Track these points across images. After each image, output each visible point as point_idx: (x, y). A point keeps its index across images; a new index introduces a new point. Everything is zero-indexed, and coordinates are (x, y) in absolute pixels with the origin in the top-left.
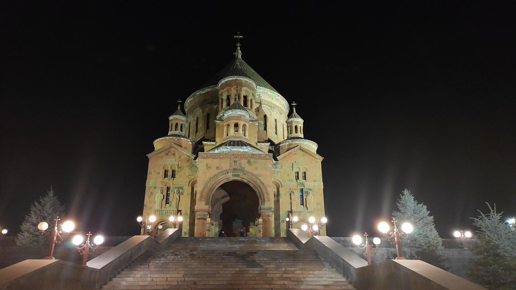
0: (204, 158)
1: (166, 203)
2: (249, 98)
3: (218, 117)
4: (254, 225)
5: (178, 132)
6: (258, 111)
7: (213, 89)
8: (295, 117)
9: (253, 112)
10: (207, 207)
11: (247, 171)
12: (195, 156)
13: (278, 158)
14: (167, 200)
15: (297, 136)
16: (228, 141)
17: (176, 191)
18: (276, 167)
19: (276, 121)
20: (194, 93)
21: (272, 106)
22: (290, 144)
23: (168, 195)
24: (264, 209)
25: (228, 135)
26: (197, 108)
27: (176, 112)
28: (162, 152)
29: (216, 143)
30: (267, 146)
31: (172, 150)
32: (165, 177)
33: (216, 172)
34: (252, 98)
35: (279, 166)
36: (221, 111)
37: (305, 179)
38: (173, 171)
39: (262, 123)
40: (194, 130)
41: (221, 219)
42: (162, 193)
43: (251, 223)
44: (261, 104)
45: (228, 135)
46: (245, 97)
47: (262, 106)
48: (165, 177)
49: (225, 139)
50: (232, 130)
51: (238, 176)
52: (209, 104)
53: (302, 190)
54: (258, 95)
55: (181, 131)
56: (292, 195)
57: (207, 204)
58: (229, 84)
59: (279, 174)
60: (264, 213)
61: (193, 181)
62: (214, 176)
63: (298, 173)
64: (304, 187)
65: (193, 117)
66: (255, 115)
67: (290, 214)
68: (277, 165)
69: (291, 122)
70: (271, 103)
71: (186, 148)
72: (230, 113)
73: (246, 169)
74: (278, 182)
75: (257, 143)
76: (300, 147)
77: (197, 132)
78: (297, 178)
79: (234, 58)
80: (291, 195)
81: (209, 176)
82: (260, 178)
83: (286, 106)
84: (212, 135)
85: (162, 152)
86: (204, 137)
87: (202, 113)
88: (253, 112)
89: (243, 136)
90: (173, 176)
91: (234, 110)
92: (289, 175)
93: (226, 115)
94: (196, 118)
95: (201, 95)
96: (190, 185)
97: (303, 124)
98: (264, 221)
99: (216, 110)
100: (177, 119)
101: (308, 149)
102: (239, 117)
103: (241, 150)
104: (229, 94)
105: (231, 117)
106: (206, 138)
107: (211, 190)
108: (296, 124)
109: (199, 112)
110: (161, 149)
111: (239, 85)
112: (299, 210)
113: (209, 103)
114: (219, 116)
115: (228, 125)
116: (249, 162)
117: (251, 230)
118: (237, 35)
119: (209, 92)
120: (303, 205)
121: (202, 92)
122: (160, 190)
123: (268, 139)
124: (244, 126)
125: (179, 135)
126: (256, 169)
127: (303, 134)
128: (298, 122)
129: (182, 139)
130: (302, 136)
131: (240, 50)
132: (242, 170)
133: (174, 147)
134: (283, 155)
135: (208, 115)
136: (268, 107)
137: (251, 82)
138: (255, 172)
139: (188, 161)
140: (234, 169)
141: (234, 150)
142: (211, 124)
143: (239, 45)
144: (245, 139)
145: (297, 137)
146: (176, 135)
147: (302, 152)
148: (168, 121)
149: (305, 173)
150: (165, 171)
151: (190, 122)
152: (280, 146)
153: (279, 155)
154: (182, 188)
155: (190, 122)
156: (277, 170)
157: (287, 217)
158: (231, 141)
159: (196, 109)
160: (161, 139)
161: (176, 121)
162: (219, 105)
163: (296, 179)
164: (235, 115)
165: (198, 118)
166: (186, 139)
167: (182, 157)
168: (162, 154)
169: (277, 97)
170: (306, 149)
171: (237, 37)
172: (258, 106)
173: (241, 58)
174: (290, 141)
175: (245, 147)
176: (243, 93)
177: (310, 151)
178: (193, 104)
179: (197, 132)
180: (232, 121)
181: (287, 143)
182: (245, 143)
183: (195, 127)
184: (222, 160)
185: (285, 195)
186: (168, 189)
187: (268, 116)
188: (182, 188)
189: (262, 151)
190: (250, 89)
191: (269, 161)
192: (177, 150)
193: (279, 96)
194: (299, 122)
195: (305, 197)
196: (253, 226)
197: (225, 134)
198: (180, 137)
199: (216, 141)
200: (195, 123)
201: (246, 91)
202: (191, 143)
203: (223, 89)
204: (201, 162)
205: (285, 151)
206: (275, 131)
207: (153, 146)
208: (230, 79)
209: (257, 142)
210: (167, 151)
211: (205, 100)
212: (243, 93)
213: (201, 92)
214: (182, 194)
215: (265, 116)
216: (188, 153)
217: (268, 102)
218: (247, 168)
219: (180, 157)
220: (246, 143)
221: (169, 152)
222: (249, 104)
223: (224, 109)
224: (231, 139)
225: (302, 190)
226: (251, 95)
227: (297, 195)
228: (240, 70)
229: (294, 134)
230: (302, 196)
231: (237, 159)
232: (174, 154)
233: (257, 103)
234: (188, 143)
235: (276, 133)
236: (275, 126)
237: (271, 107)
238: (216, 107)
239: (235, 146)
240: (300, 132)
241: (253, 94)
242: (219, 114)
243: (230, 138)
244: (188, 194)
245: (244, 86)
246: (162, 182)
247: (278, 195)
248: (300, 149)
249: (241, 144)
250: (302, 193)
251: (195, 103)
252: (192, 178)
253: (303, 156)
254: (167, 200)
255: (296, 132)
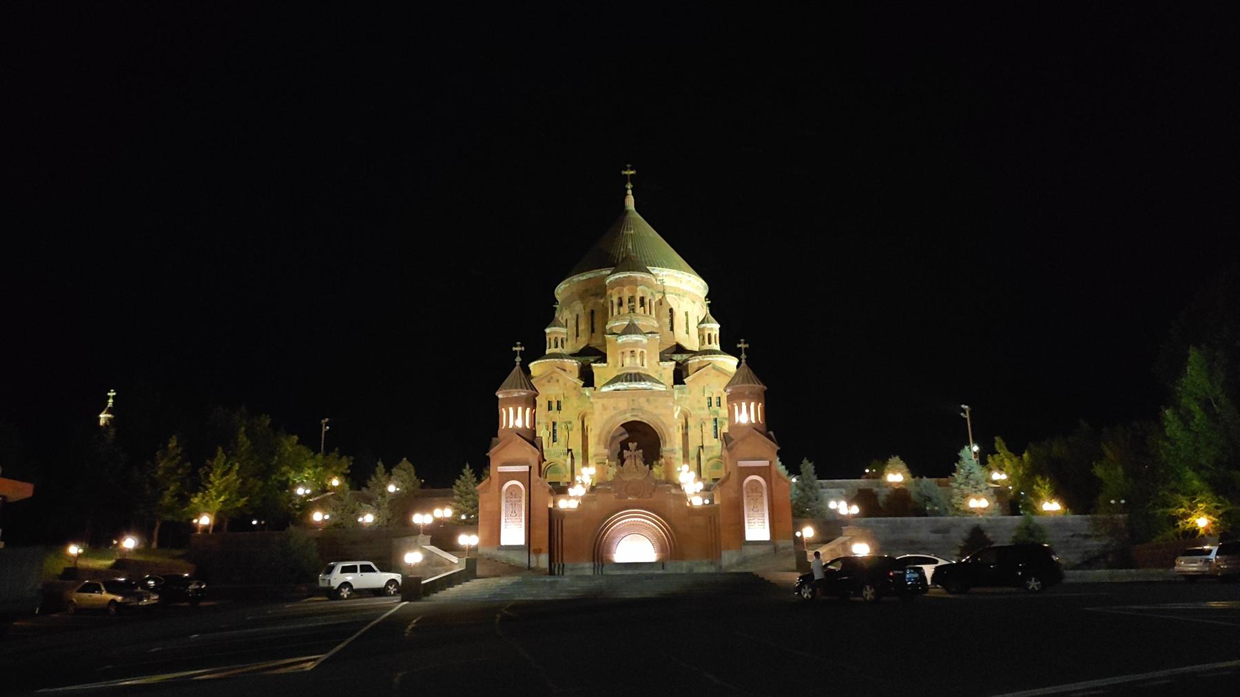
0: (600, 398)
1: (554, 441)
2: (647, 301)
3: (608, 327)
4: (658, 464)
5: (558, 350)
6: (661, 304)
7: (598, 275)
8: (708, 323)
9: (653, 318)
10: (606, 451)
11: (646, 411)
12: (583, 382)
13: (685, 380)
14: (554, 436)
15: (711, 348)
16: (624, 374)
17: (563, 427)
18: (683, 393)
19: (686, 314)
20: (569, 279)
21: (680, 294)
22: (700, 362)
23: (554, 431)
24: (666, 451)
25: (623, 366)
26: (576, 300)
27: (553, 322)
28: (543, 378)
29: (608, 365)
30: (672, 365)
31: (553, 375)
32: (549, 410)
33: (613, 413)
34: (651, 297)
35: (687, 391)
36: (610, 320)
37: (720, 406)
38: (558, 402)
39: (667, 320)
40: (573, 333)
41: (619, 458)
42: (547, 429)
43: (655, 462)
44: (664, 293)
45: (623, 366)
46: (642, 299)
47: (666, 296)
48: (549, 410)
49: (619, 371)
50: (628, 361)
51: (637, 416)
52: (592, 298)
53: (716, 420)
54: (660, 280)
55: (563, 347)
56: (703, 427)
57: (605, 448)
58: (619, 283)
59: (688, 402)
60: (664, 454)
61: (583, 413)
62: (612, 417)
63: (710, 398)
64: (718, 415)
65: (571, 314)
66: (656, 322)
67: (701, 450)
68: (684, 390)
69: (703, 328)
70: (679, 289)
71: (570, 372)
72: (624, 339)
73: (645, 409)
74: (687, 411)
75: (658, 363)
76: (714, 365)
77: (577, 336)
78: (710, 405)
79: (623, 210)
80: (702, 427)
81: (605, 417)
82: (661, 417)
83: (702, 287)
84: (599, 341)
85: (543, 378)
86: (588, 344)
87: (584, 309)
88: (653, 318)
89: (640, 366)
90: (559, 408)
91: (629, 336)
92: (699, 402)
93: (620, 341)
94: (575, 317)
95: (579, 282)
96: (580, 418)
97: (718, 330)
98: (666, 462)
99: (603, 305)
100: (556, 332)
101: (723, 367)
102: (636, 343)
103: (639, 386)
104: (620, 296)
105: (624, 344)
106: (592, 346)
107: (609, 432)
108: (709, 332)
109: (578, 307)
110: (540, 376)
111: (634, 283)
112: (712, 444)
113: (593, 295)
114: (610, 327)
115: (623, 353)
116: (648, 400)
117: (654, 469)
118: (626, 170)
119: (590, 278)
120: (717, 438)
121: (581, 278)
122: (544, 427)
123: (675, 344)
124: (642, 352)
125: (560, 354)
126: (656, 407)
127: (719, 345)
128: (712, 329)
129: (566, 360)
130: (717, 347)
131: (633, 194)
132: (641, 409)
133: (557, 373)
134: (691, 376)
135: (593, 312)
136: (675, 297)
137: (648, 277)
138: (655, 411)
139: (575, 389)
140: (633, 409)
141: (631, 386)
142: (596, 326)
143: (629, 186)
144: (645, 370)
145: (709, 350)
146: (557, 354)
147: (715, 372)
148: (545, 333)
149: (719, 398)
150: (549, 402)
151: (566, 320)
152: (687, 365)
153: (688, 376)
154: (570, 423)
155: (566, 320)
156: (684, 396)
157: (684, 463)
158: (627, 374)
159: (575, 302)
160: (539, 361)
161: (555, 336)
162: (606, 299)
163: (709, 407)
164: (631, 341)
165: (577, 316)
166: (570, 361)
167: (568, 384)
168: (543, 382)
169: (689, 279)
170: (722, 369)
171: (626, 173)
172: (660, 297)
173: (634, 209)
174: (700, 357)
175: (643, 383)
176: (639, 295)
177: (725, 370)
178: (569, 294)
179: (577, 336)
180: (627, 349)
181: (697, 360)
182: (643, 376)
183: (575, 329)
184: (620, 399)
185: (695, 427)
186: (554, 424)
187: (675, 310)
188: (570, 423)
189: (662, 384)
190: (648, 288)
191: (669, 398)
192: (561, 375)
193: (690, 276)
194: (714, 328)
195: (719, 429)
196: (657, 466)
197: (620, 364)
198: (562, 358)
199: (608, 361)
200: (574, 322)
201: (643, 291)
202: (576, 364)
203: (613, 289)
204: (597, 402)
205: (695, 370)
206: (685, 329)
207: (529, 368)
208: (622, 276)
209: (659, 360)
210: (549, 378)
211: (586, 291)
212: (639, 295)
213: (580, 278)
214: (572, 430)
215: (671, 310)
216: (574, 379)
217: (675, 288)
218: (647, 407)
219: (565, 384)
220: (645, 375)
221: (552, 378)
222: (647, 307)
223: (616, 316)
224: (627, 371)
225: (716, 420)
226: (649, 294)
227: (709, 426)
228: (632, 259)
229: (707, 346)
230: (716, 427)
231: (635, 398)
232: (558, 381)
233: (659, 292)
234: (573, 364)
235: (687, 333)
236: (685, 322)
237: (679, 295)
238: (602, 301)
239: (631, 381)
240: (715, 342)
241: (652, 293)
242: (609, 323)
243: (623, 370)
244: (578, 430)
245: (641, 285)
246: (546, 416)
247: (687, 427)
248: (714, 368)
249: (638, 377)
250: (716, 423)
251: (572, 293)
252: (582, 409)
253: (718, 376)
254: (554, 437)
255: (710, 343)
